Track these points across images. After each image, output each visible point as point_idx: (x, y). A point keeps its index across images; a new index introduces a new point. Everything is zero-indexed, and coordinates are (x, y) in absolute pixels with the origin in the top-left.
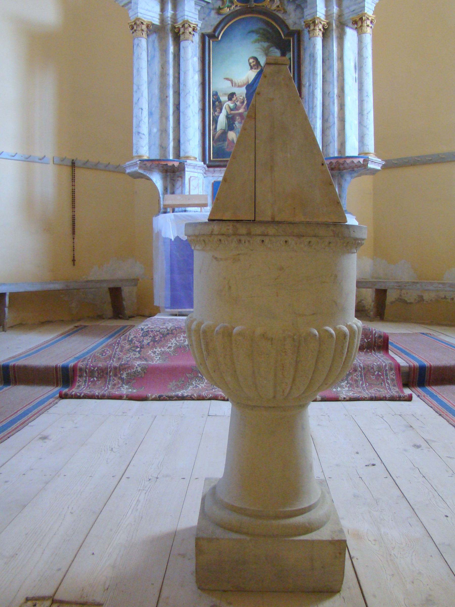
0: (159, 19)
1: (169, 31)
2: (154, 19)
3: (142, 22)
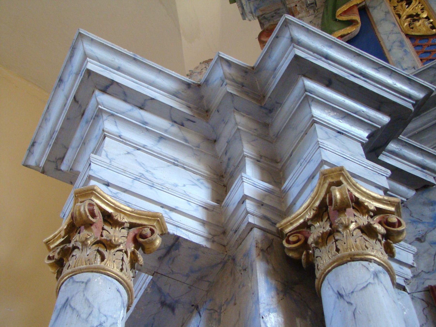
0: (203, 223)
1: (254, 252)
2: (175, 216)
3: (110, 210)
